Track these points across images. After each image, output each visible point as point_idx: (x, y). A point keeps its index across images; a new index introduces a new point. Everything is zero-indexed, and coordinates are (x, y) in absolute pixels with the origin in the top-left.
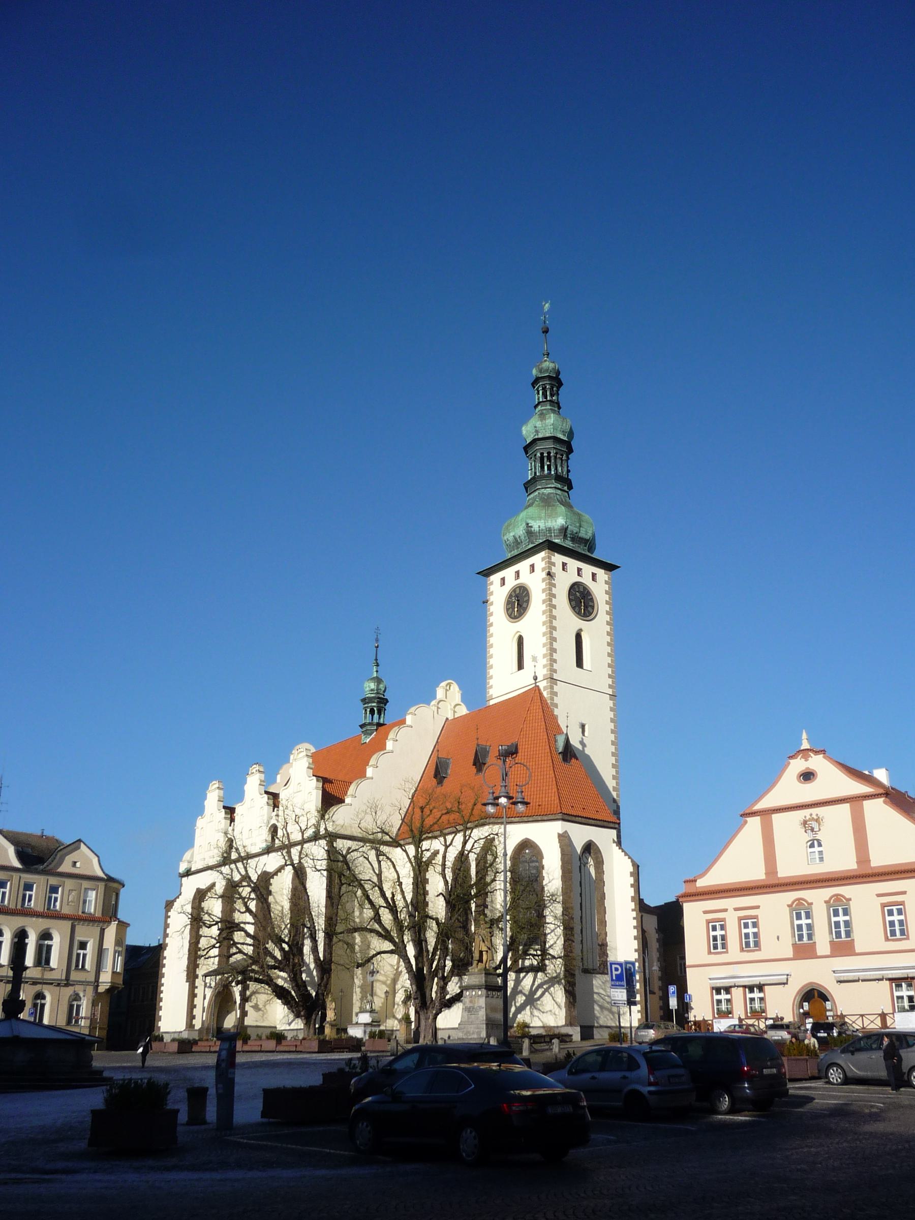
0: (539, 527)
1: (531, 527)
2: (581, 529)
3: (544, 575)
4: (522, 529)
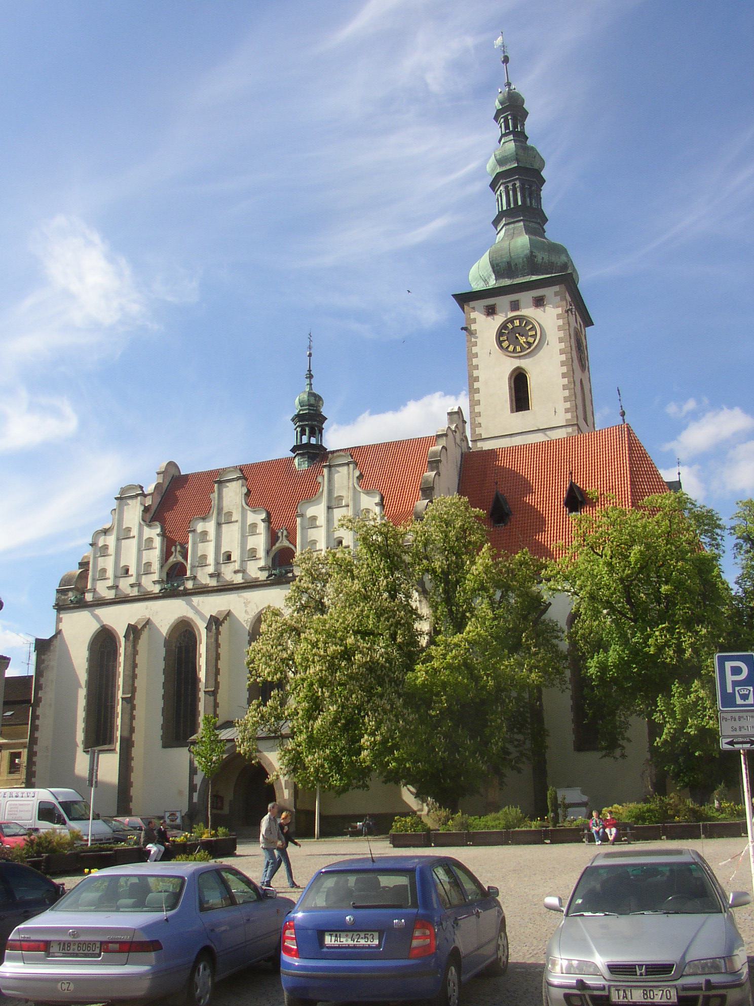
1: (535, 257)
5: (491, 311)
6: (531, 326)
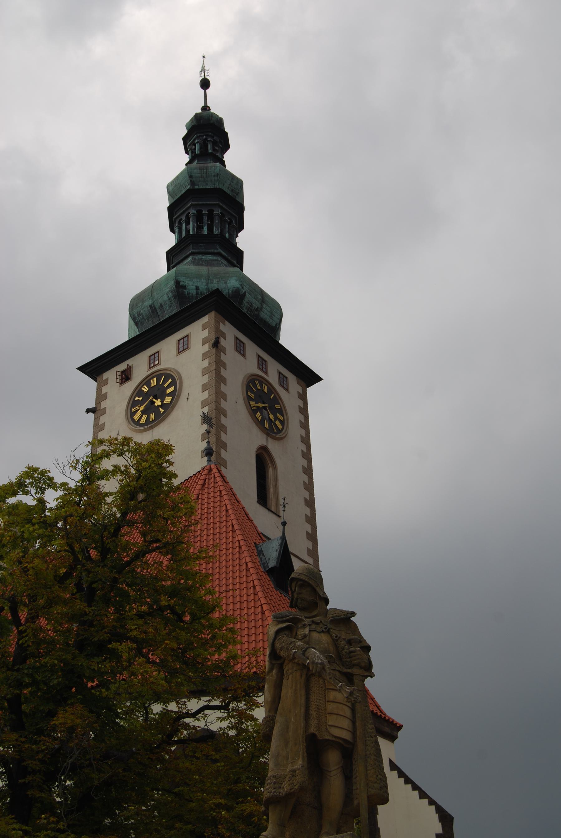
0: (197, 288)
1: (184, 287)
2: (264, 305)
3: (206, 347)
4: (167, 291)
5: (125, 377)
6: (170, 380)
